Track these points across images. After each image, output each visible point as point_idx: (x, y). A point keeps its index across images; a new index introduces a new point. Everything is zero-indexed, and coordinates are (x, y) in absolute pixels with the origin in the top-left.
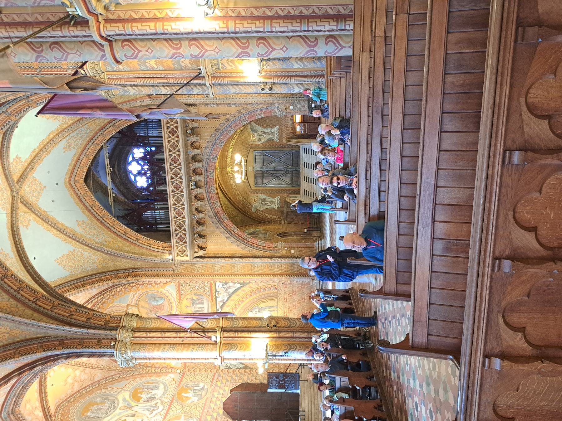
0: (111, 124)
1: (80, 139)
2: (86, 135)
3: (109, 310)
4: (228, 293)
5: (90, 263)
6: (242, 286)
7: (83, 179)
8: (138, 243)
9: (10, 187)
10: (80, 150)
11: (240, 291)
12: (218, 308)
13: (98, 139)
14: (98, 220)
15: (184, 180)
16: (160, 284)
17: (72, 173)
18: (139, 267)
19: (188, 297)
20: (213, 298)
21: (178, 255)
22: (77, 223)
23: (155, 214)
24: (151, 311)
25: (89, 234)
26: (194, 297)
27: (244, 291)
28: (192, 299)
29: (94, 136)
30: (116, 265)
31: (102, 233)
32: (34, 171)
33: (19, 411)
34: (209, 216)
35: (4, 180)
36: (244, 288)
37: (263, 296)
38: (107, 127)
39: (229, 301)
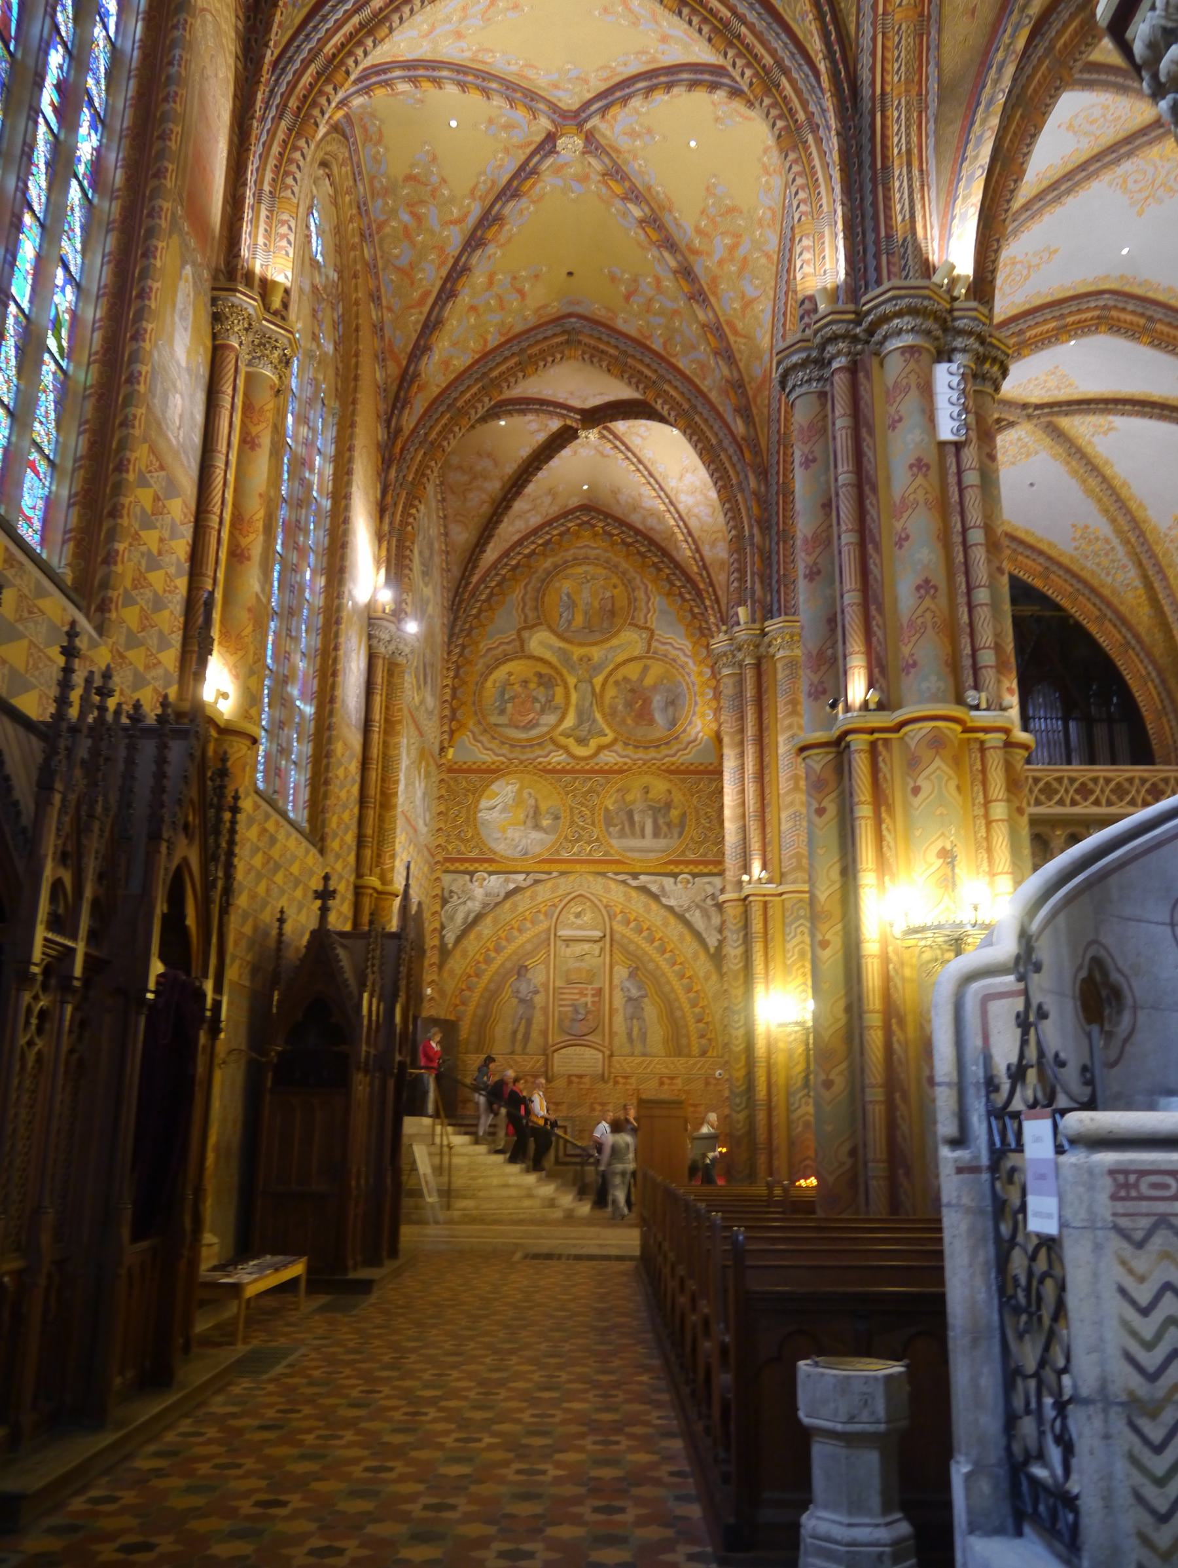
0: (1133, 642)
1: (1098, 564)
2: (1109, 580)
3: (638, 581)
4: (688, 910)
6: (712, 950)
9: (1051, 405)
10: (1065, 561)
11: (695, 945)
12: (642, 877)
13: (1089, 606)
16: (717, 719)
19: (677, 797)
24: (632, 691)
26: (674, 813)
27: (696, 957)
28: (668, 805)
32: (1054, 456)
33: (569, 358)
35: (1076, 396)
36: (702, 956)
37: (678, 1013)
39: (663, 912)
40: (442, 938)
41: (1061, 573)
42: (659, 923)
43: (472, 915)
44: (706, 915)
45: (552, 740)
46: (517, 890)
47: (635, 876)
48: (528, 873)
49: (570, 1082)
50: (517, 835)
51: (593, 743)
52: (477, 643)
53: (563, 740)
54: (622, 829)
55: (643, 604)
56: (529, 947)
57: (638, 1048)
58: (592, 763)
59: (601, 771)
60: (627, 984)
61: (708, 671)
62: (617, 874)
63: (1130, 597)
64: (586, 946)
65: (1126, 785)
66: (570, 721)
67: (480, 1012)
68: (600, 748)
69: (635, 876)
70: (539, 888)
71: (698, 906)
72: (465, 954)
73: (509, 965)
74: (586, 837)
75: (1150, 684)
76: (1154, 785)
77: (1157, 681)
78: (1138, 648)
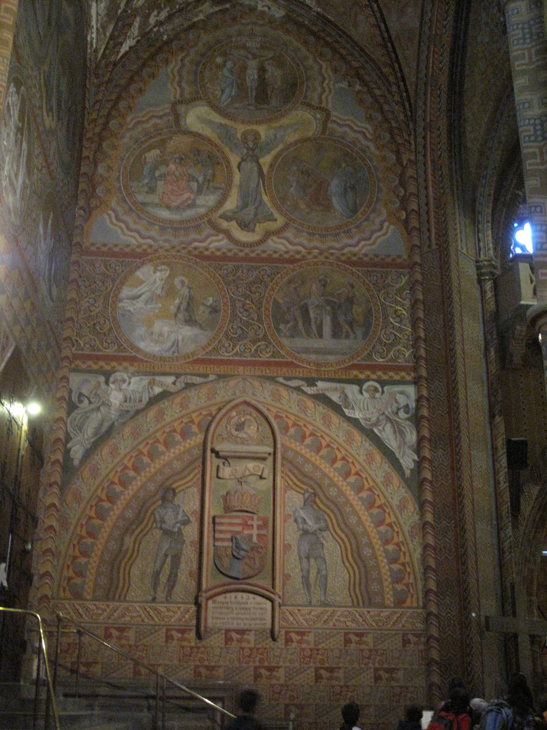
4: (376, 424)
6: (408, 473)
11: (387, 467)
12: (320, 384)
20: (355, 372)
26: (358, 310)
27: (387, 482)
28: (350, 301)
37: (367, 552)
40: (67, 452)
42: (341, 440)
43: (106, 425)
44: (399, 431)
45: (210, 222)
46: (165, 395)
47: (311, 382)
48: (178, 376)
49: (228, 640)
50: (166, 329)
51: (260, 228)
52: (124, 117)
53: (225, 224)
54: (296, 326)
55: (317, 83)
56: (177, 465)
57: (318, 595)
58: (258, 250)
59: (269, 260)
60: (302, 514)
61: (393, 157)
62: (287, 379)
64: (251, 465)
66: (231, 204)
67: (113, 546)
68: (268, 234)
69: (311, 382)
70: (192, 393)
71: (388, 419)
72: (95, 472)
73: (152, 487)
74: (251, 334)
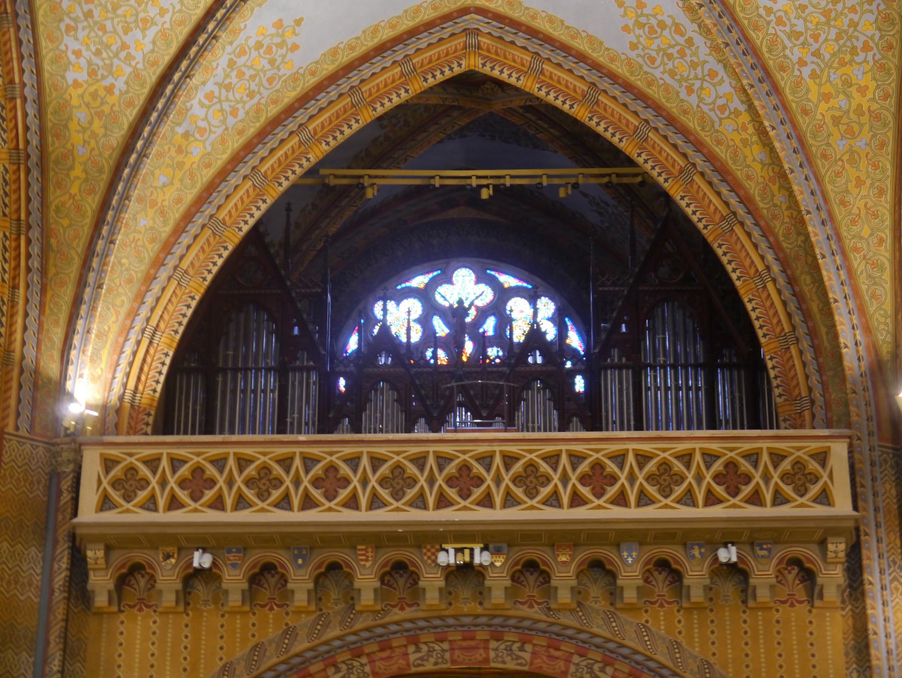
0: (741, 211)
1: (672, 74)
2: (693, 99)
5: (98, 53)
7: (479, 68)
8: (163, 274)
10: (621, 70)
14: (290, 111)
15: (498, 514)
17: (516, 25)
18: (52, 271)
21: (108, 464)
22: (288, 22)
23: (258, 370)
25: (231, 64)
29: (685, 132)
30: (72, 168)
31: (231, 121)
34: (290, 633)
38: (724, 190)
41: (617, 92)
63: (728, 128)
65: (678, 466)
75: (770, 286)
76: (731, 465)
77: (781, 281)
78: (749, 221)
